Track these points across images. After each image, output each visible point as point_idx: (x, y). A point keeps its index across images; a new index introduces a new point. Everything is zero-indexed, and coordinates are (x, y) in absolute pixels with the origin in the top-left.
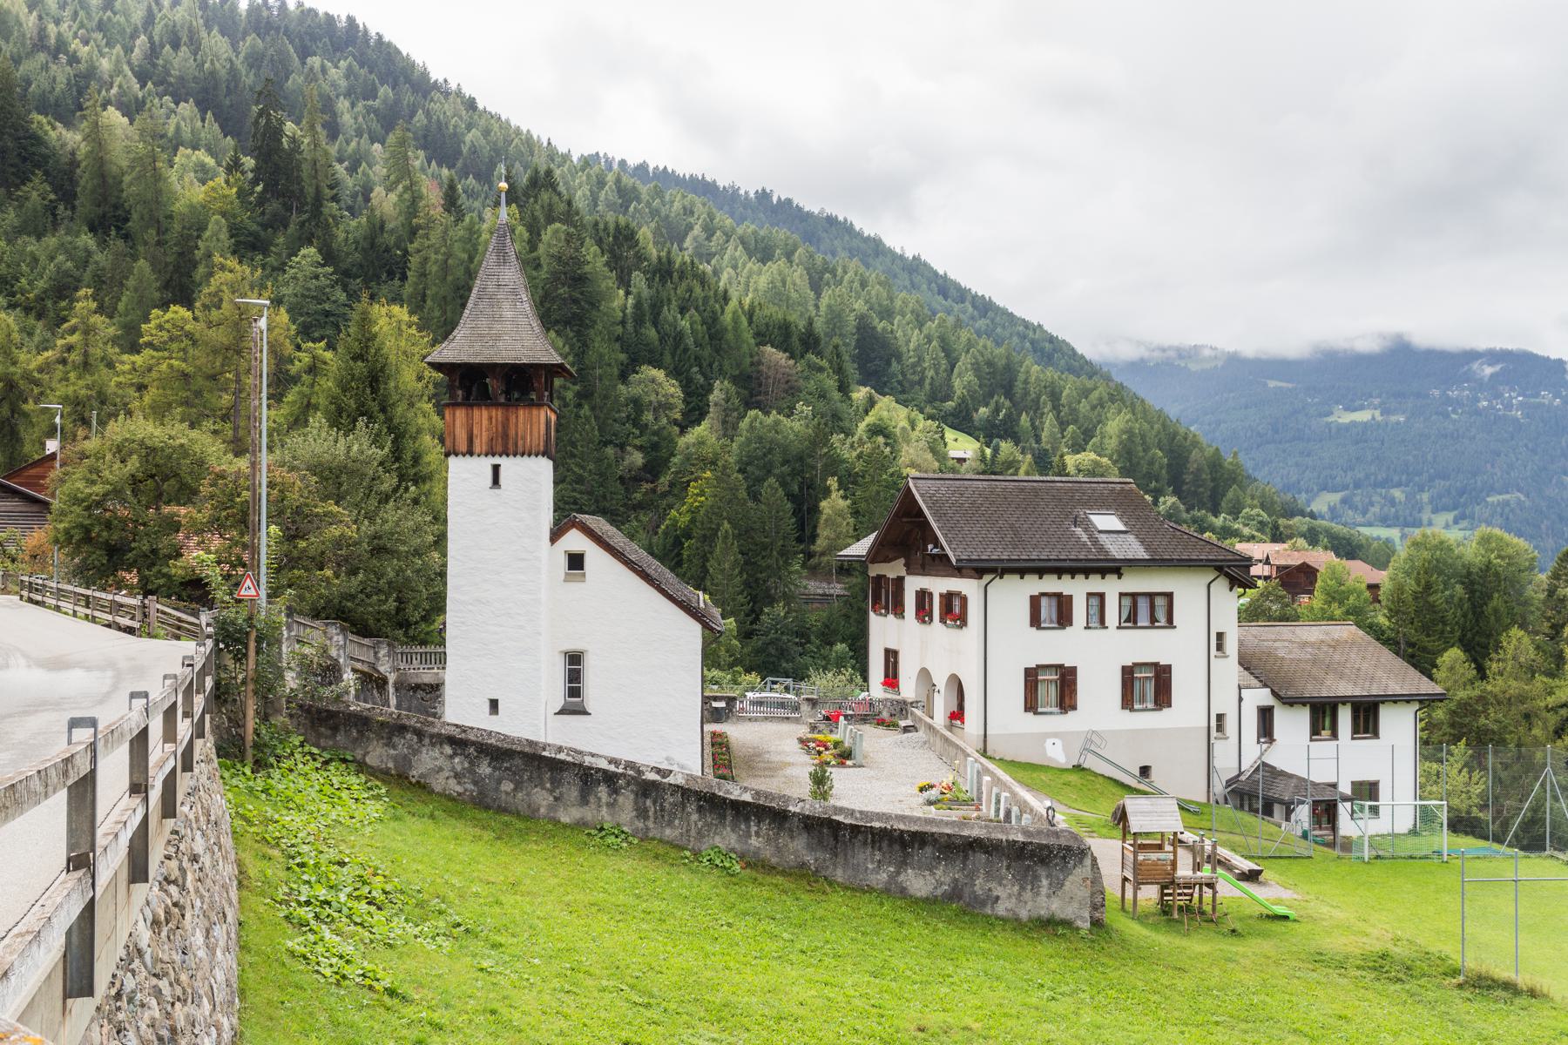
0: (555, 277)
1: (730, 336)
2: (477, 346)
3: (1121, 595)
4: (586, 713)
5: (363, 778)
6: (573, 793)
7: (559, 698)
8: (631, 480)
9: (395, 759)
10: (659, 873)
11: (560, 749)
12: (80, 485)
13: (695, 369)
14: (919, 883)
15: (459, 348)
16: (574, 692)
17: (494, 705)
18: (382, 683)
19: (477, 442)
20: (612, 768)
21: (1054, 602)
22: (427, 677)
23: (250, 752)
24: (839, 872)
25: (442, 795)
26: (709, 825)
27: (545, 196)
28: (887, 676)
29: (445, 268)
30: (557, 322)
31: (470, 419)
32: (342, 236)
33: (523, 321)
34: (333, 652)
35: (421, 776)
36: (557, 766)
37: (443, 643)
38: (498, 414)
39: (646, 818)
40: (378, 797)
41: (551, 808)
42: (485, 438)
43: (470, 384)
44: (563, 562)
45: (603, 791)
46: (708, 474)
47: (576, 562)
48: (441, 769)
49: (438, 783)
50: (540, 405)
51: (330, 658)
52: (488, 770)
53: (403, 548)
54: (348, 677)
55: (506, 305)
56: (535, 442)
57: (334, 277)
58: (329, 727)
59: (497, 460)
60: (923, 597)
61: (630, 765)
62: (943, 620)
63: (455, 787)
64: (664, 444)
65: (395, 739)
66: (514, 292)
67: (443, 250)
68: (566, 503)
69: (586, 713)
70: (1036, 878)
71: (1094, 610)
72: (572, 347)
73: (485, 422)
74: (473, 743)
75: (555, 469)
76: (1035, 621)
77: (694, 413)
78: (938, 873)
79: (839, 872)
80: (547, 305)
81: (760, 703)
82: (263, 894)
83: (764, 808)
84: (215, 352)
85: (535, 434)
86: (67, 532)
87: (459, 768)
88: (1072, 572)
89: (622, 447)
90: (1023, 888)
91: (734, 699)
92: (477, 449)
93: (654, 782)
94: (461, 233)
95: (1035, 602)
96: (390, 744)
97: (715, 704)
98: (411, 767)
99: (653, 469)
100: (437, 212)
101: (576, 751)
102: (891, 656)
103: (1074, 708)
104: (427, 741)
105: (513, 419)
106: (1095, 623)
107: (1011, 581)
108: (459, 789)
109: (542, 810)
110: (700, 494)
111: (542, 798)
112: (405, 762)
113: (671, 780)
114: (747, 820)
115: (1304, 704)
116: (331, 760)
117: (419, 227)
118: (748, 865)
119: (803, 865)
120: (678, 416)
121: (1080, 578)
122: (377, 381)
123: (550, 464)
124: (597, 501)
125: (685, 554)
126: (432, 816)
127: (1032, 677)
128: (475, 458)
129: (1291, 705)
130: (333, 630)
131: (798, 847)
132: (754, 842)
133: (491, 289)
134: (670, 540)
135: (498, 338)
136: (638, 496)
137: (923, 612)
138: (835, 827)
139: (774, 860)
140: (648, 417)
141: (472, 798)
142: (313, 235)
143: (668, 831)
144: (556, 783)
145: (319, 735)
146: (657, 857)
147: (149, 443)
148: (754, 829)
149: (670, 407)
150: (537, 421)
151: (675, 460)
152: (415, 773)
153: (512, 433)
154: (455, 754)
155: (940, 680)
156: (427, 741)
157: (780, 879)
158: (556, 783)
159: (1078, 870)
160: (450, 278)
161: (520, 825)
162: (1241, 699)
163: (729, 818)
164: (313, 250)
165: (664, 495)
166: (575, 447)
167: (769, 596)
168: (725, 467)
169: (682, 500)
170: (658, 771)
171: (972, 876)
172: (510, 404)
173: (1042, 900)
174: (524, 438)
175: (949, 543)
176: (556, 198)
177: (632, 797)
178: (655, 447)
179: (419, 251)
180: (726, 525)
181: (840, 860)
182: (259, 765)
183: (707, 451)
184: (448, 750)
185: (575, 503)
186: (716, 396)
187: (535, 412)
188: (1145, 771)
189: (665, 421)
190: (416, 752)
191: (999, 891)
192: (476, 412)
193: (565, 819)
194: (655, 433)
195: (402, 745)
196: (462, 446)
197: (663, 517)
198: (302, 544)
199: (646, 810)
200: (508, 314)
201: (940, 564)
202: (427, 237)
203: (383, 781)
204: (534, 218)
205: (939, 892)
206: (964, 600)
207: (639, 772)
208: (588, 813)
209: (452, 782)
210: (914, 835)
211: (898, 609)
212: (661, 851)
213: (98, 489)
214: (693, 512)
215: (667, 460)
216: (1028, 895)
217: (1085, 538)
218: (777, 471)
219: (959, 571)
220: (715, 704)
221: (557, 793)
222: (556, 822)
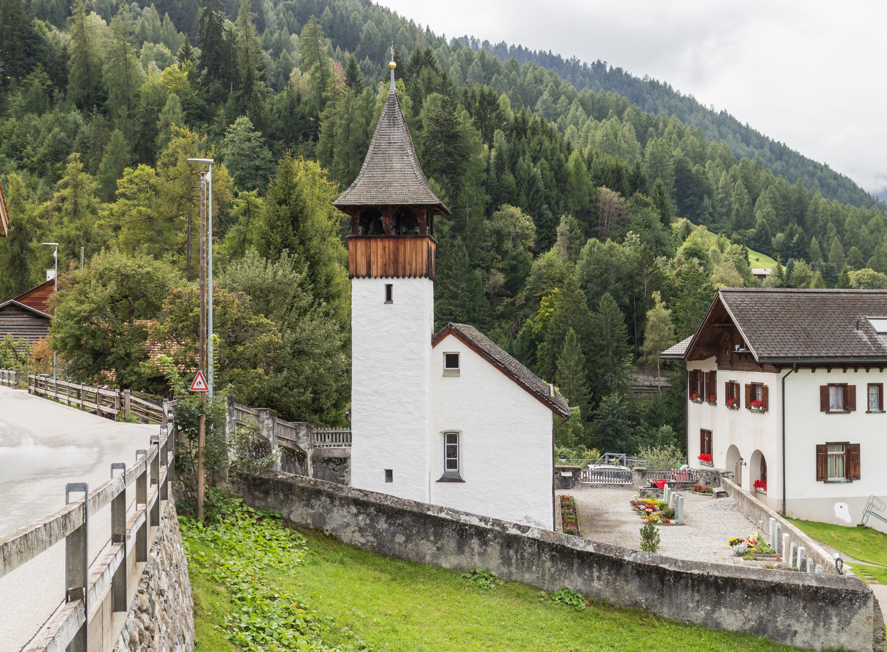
0: (434, 136)
1: (573, 180)
4: (461, 481)
5: (288, 531)
6: (452, 545)
7: (440, 470)
8: (495, 296)
9: (313, 516)
10: (519, 608)
11: (441, 509)
12: (73, 304)
13: (545, 206)
14: (731, 619)
15: (359, 193)
17: (389, 474)
19: (374, 267)
20: (482, 524)
21: (840, 391)
22: (337, 453)
23: (202, 511)
24: (665, 610)
25: (349, 545)
26: (560, 571)
27: (425, 72)
28: (702, 451)
29: (348, 130)
30: (435, 170)
31: (368, 248)
32: (268, 107)
34: (265, 433)
35: (333, 530)
37: (349, 425)
38: (390, 244)
39: (510, 564)
40: (300, 547)
41: (434, 556)
42: (380, 264)
43: (368, 221)
44: (442, 361)
45: (475, 543)
46: (556, 290)
47: (452, 361)
48: (348, 525)
49: (346, 536)
50: (423, 237)
51: (263, 437)
52: (385, 526)
55: (396, 159)
57: (262, 140)
58: (261, 491)
59: (389, 281)
60: (732, 387)
61: (496, 522)
62: (748, 406)
63: (359, 539)
64: (521, 266)
65: (313, 501)
66: (402, 148)
67: (346, 116)
68: (444, 314)
69: (461, 481)
70: (828, 616)
71: (874, 398)
72: (447, 190)
73: (380, 252)
74: (373, 504)
75: (435, 287)
76: (825, 407)
77: (546, 241)
78: (747, 611)
79: (665, 610)
80: (428, 158)
81: (600, 473)
82: (212, 621)
83: (604, 557)
84: (173, 200)
85: (419, 259)
86: (63, 340)
87: (362, 524)
88: (856, 366)
89: (487, 269)
90: (816, 625)
91: (579, 470)
92: (374, 273)
93: (515, 536)
95: (824, 392)
96: (308, 505)
97: (564, 474)
98: (325, 523)
99: (512, 287)
100: (341, 86)
101: (454, 511)
102: (706, 436)
103: (858, 477)
104: (337, 502)
105: (402, 248)
106: (874, 407)
107: (804, 375)
108: (363, 540)
109: (428, 558)
110: (549, 308)
111: (427, 548)
112: (321, 519)
113: (529, 534)
114: (590, 567)
116: (264, 517)
117: (327, 99)
118: (592, 603)
119: (636, 604)
120: (532, 244)
121: (862, 371)
122: (297, 221)
124: (468, 313)
125: (539, 353)
126: (342, 562)
127: (822, 452)
128: (373, 279)
130: (264, 416)
131: (632, 590)
132: (596, 584)
133: (384, 145)
134: (528, 343)
135: (389, 184)
136: (501, 308)
137: (732, 400)
138: (662, 573)
139: (612, 600)
140: (508, 245)
141: (373, 548)
142: (246, 107)
143: (527, 576)
144: (438, 536)
145: (255, 498)
146: (518, 596)
147: (123, 271)
148: (596, 574)
149: (525, 237)
150: (420, 250)
151: (530, 279)
152: (328, 528)
153: (401, 259)
154: (359, 513)
155: (747, 455)
156: (337, 502)
157: (617, 615)
158: (438, 536)
159: (863, 610)
160: (351, 138)
161: (410, 569)
163: (576, 566)
164: (246, 119)
165: (521, 307)
166: (451, 270)
167: (606, 388)
168: (569, 285)
169: (535, 311)
170: (519, 527)
171: (774, 614)
172: (399, 236)
173: (833, 634)
174: (410, 264)
175: (753, 343)
176: (434, 74)
177: (498, 548)
178: (514, 269)
179: (327, 118)
181: (666, 600)
182: (209, 521)
183: (555, 272)
184: (354, 510)
185: (451, 314)
186: (562, 228)
187: (419, 242)
189: (522, 248)
190: (329, 511)
191: (796, 627)
192: (373, 243)
193: (446, 565)
194: (514, 258)
195: (318, 505)
196: (363, 270)
197: (520, 325)
198: (240, 348)
199: (509, 559)
200: (397, 165)
201: (745, 361)
203: (304, 534)
204: (417, 90)
205: (747, 627)
206: (766, 390)
207: (504, 528)
208: (463, 560)
209: (357, 535)
210: (727, 580)
211: (712, 398)
212: (522, 590)
213: (86, 307)
214: (545, 320)
215: (523, 279)
216: (821, 630)
217: (865, 338)
218: (611, 287)
219: (761, 366)
220: (564, 474)
221: (439, 545)
222: (439, 567)
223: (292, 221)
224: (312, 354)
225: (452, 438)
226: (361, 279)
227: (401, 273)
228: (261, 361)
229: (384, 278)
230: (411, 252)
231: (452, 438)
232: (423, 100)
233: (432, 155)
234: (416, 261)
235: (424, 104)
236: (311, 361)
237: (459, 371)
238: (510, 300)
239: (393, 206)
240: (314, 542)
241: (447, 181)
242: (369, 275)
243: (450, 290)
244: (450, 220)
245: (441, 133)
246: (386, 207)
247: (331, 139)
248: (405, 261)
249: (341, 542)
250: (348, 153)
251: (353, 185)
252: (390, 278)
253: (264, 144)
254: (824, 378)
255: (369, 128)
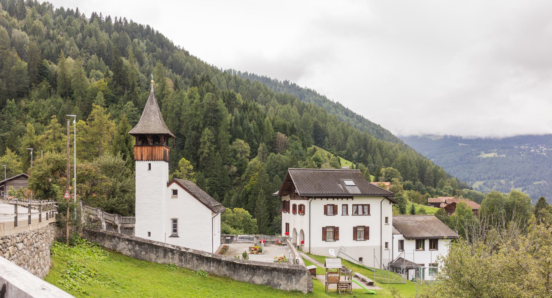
0: (208, 111)
1: (266, 129)
3: (353, 205)
4: (178, 237)
7: (170, 232)
9: (112, 245)
10: (183, 276)
11: (158, 243)
12: (36, 171)
13: (254, 140)
14: (258, 280)
16: (175, 231)
17: (149, 233)
18: (116, 227)
19: (144, 157)
20: (173, 248)
21: (332, 207)
22: (130, 226)
23: (68, 241)
24: (236, 277)
25: (125, 255)
26: (199, 264)
27: (206, 84)
28: (286, 231)
29: (173, 108)
30: (209, 125)
31: (141, 150)
33: (157, 121)
34: (99, 217)
36: (157, 247)
37: (134, 215)
39: (182, 262)
40: (106, 255)
41: (155, 259)
43: (144, 139)
45: (170, 254)
47: (175, 192)
48: (125, 248)
49: (124, 252)
50: (162, 146)
52: (138, 248)
53: (130, 190)
54: (104, 224)
58: (94, 235)
59: (150, 162)
60: (294, 206)
61: (178, 247)
62: (299, 213)
63: (129, 253)
66: (155, 113)
69: (178, 237)
70: (292, 279)
71: (345, 210)
72: (214, 132)
73: (146, 151)
74: (134, 241)
75: (169, 165)
76: (326, 213)
77: (254, 154)
78: (264, 277)
79: (236, 277)
82: (57, 271)
84: (93, 135)
86: (32, 185)
88: (338, 198)
89: (230, 165)
90: (288, 282)
92: (144, 159)
93: (184, 252)
94: (178, 96)
95: (326, 207)
96: (111, 241)
99: (240, 172)
100: (171, 89)
102: (287, 225)
103: (338, 239)
105: (154, 150)
106: (345, 213)
107: (318, 200)
108: (130, 254)
110: (253, 181)
111: (153, 256)
112: (115, 246)
113: (189, 251)
114: (210, 262)
115: (413, 239)
118: (210, 275)
119: (225, 275)
120: (248, 155)
121: (340, 200)
124: (221, 183)
125: (249, 199)
126: (121, 261)
127: (324, 230)
129: (409, 239)
130: (99, 210)
131: (224, 270)
132: (212, 268)
134: (245, 195)
136: (235, 181)
137: (294, 212)
138: (234, 264)
139: (218, 274)
140: (239, 155)
141: (134, 256)
143: (188, 266)
144: (157, 252)
145: (92, 239)
146: (184, 272)
147: (56, 159)
148: (212, 265)
149: (246, 152)
151: (247, 169)
153: (154, 154)
155: (298, 232)
157: (218, 279)
158: (157, 252)
159: (304, 277)
160: (174, 111)
161: (146, 263)
162: (393, 238)
164: (131, 102)
165: (243, 181)
167: (276, 213)
168: (261, 171)
169: (248, 182)
170: (186, 249)
171: (273, 278)
172: (154, 145)
173: (293, 285)
175: (298, 189)
176: (210, 84)
178: (241, 165)
180: (262, 190)
181: (236, 273)
182: (71, 245)
183: (257, 166)
184: (127, 243)
185: (214, 183)
186: (260, 148)
187: (160, 148)
188: (361, 259)
189: (244, 157)
190: (118, 243)
191: (281, 283)
192: (143, 148)
193: (159, 262)
194: (241, 161)
196: (140, 158)
197: (242, 188)
198: (96, 188)
201: (296, 196)
204: (202, 91)
205: (264, 283)
206: (304, 206)
207: (180, 249)
208: (166, 260)
209: (128, 252)
210: (257, 266)
211: (288, 210)
212: (185, 270)
213: (41, 173)
214: (252, 186)
215: (244, 170)
216: (289, 284)
217: (341, 187)
218: (279, 173)
219: (303, 197)
222: (157, 263)
225: (175, 221)
231: (175, 221)
238: (238, 178)
240: (112, 254)
242: (142, 160)
246: (148, 134)
249: (122, 254)
254: (325, 202)
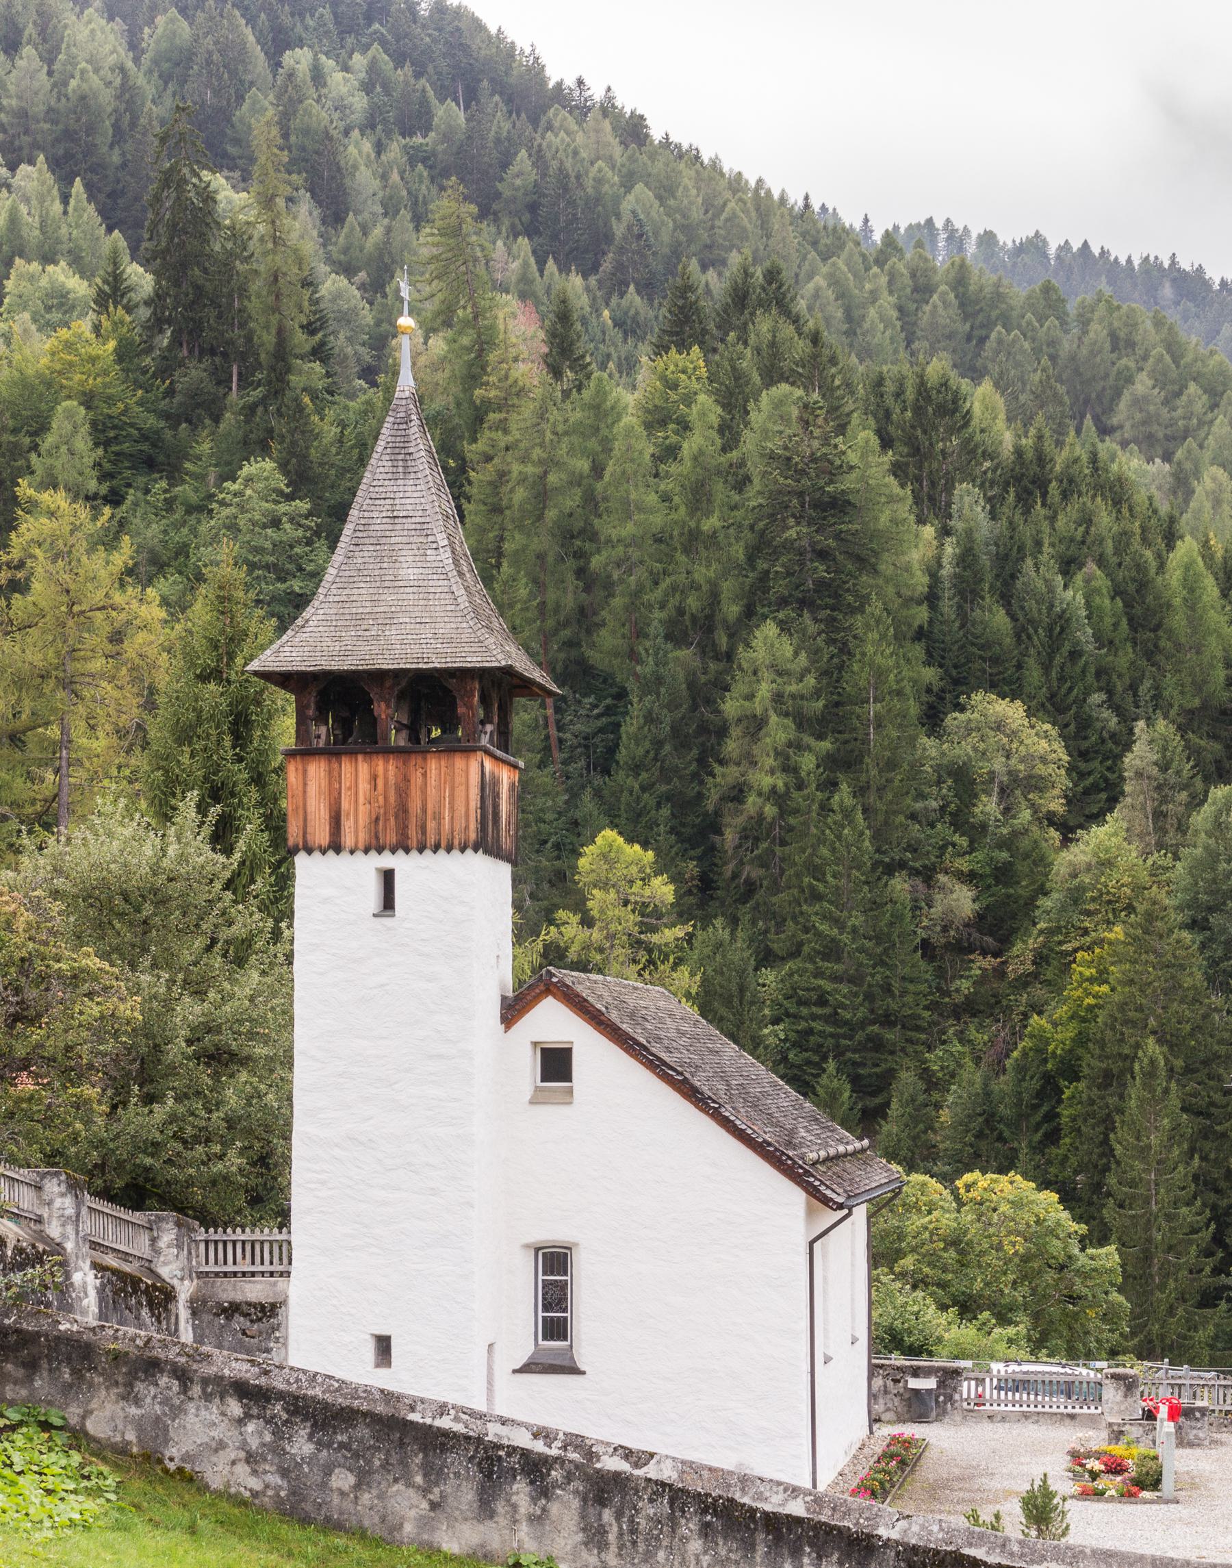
1: (1178, 621)
2: (348, 638)
4: (573, 1370)
5: (76, 1458)
6: (465, 1495)
7: (522, 1339)
8: (946, 951)
9: (139, 1425)
11: (443, 1409)
13: (1097, 698)
16: (556, 1329)
17: (383, 1346)
18: (160, 1298)
19: (347, 825)
20: (539, 1447)
22: (254, 1291)
25: (224, 1495)
27: (764, 325)
29: (542, 495)
30: (783, 602)
31: (334, 778)
32: (332, 432)
34: (54, 1230)
35: (187, 1457)
36: (435, 1442)
37: (283, 1217)
38: (387, 769)
39: (603, 1546)
40: (96, 1492)
41: (425, 1524)
42: (363, 819)
43: (345, 706)
44: (530, 1066)
45: (520, 1491)
46: (1118, 932)
47: (556, 1064)
48: (221, 1446)
49: (217, 1473)
50: (469, 751)
51: (47, 1240)
52: (308, 1448)
53: (260, 1050)
54: (85, 1279)
55: (407, 556)
56: (459, 824)
57: (311, 523)
59: (387, 860)
61: (575, 1441)
63: (246, 1480)
64: (1022, 867)
65: (140, 1387)
67: (537, 453)
68: (801, 1003)
69: (574, 1371)
72: (815, 653)
73: (364, 786)
74: (281, 1395)
75: (516, 881)
77: (1094, 795)
80: (762, 565)
81: (1019, 1385)
83: (829, 1529)
85: (461, 810)
87: (254, 1443)
89: (927, 875)
91: (956, 1373)
92: (348, 839)
93: (617, 1475)
94: (578, 415)
96: (130, 1396)
97: (914, 1383)
98: (167, 1440)
99: (998, 924)
100: (529, 371)
101: (473, 1414)
104: (196, 1390)
105: (416, 778)
108: (255, 1484)
109: (408, 1528)
110: (1088, 984)
111: (406, 1503)
112: (156, 1431)
113: (650, 1471)
114: (796, 1553)
116: (21, 1424)
120: (1057, 805)
122: (248, 723)
123: (504, 871)
124: (869, 997)
125: (1065, 1113)
126: (192, 1530)
128: (345, 855)
130: (53, 1187)
133: (379, 524)
134: (1035, 1084)
135: (388, 620)
136: (965, 985)
140: (988, 806)
142: (270, 431)
149: (1036, 784)
150: (464, 780)
151: (1046, 903)
152: (174, 1452)
153: (415, 805)
154: (248, 1416)
156: (196, 1390)
158: (434, 1475)
160: (551, 514)
163: (761, 1549)
164: (268, 465)
165: (1024, 982)
166: (822, 879)
168: (1150, 917)
169: (1056, 987)
172: (416, 746)
174: (438, 817)
176: (788, 330)
177: (576, 1503)
178: (1003, 874)
179: (489, 459)
180: (1152, 1046)
183: (1118, 881)
184: (235, 1408)
185: (822, 1002)
186: (1140, 756)
187: (459, 762)
189: (1026, 815)
190: (177, 1412)
192: (346, 766)
193: (451, 1545)
194: (1003, 844)
195: (154, 1395)
196: (321, 835)
197: (1016, 1035)
198: (36, 1035)
199: (602, 1531)
200: (410, 573)
202: (503, 427)
203: (117, 1467)
207: (591, 1455)
209: (242, 1470)
214: (1082, 1017)
215: (1030, 904)
220: (914, 1383)
221: (435, 1496)
223: (235, 723)
224: (249, 1058)
225: (555, 1262)
226: (317, 855)
227: (414, 842)
228: (91, 1066)
229: (373, 853)
230: (439, 788)
231: (555, 1262)
232: (751, 406)
233: (776, 553)
234: (452, 809)
235: (753, 416)
236: (243, 1076)
237: (570, 1091)
238: (989, 962)
239: (397, 674)
240: (137, 1484)
241: (812, 628)
242: (336, 847)
243: (819, 934)
244: (820, 737)
245: (801, 494)
246: (379, 676)
247: (497, 518)
248: (424, 811)
249: (204, 1488)
250: (541, 557)
251: (299, 622)
252: (387, 853)
253: (317, 534)
255: (599, 486)
